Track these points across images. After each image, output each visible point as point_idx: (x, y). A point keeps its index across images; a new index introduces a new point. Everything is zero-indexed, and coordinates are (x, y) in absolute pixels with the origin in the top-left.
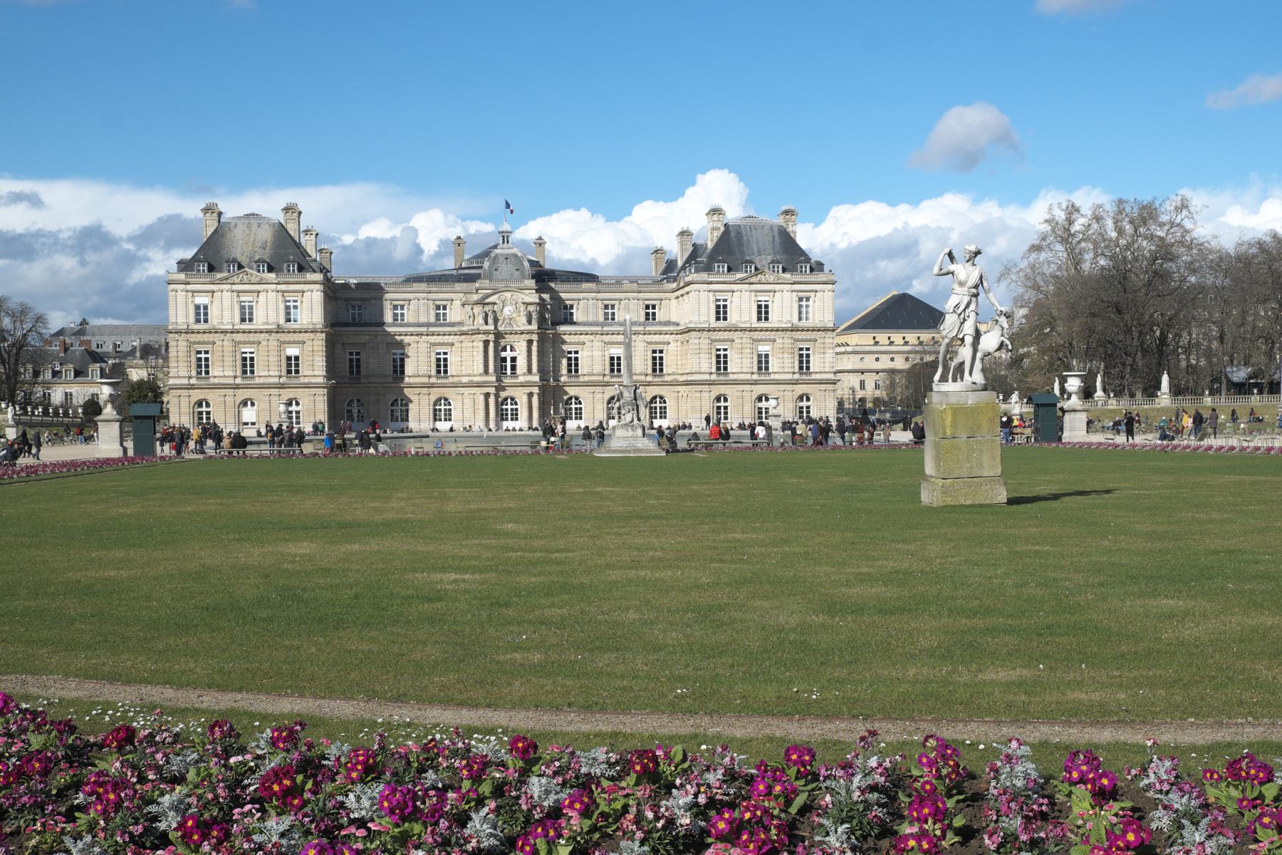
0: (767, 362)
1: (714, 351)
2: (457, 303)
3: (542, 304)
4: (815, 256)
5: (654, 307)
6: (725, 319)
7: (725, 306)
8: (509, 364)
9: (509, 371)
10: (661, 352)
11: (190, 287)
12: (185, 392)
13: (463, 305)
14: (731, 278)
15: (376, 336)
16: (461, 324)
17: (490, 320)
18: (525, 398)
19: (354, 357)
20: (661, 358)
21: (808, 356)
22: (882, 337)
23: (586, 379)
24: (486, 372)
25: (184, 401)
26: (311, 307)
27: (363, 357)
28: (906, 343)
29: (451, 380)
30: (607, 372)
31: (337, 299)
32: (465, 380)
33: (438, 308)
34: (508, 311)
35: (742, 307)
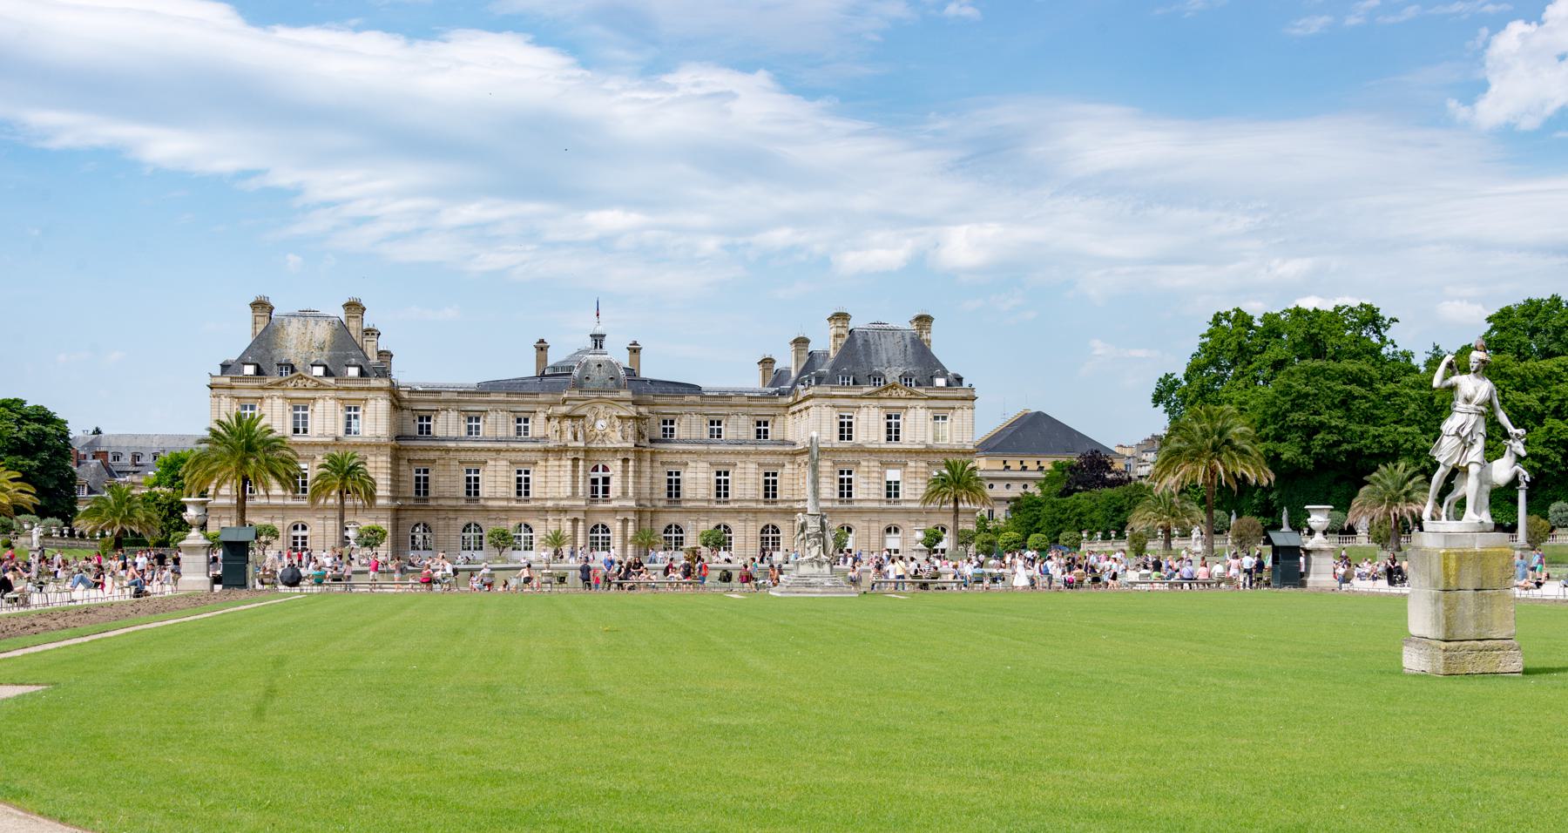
0: (897, 488)
2: (542, 416)
4: (952, 370)
5: (766, 424)
6: (850, 438)
7: (850, 424)
8: (600, 486)
9: (600, 494)
10: (775, 474)
11: (235, 393)
13: (548, 419)
14: (857, 392)
16: (546, 437)
18: (619, 524)
19: (422, 475)
20: (774, 482)
22: (1014, 464)
24: (574, 495)
26: (375, 421)
27: (431, 475)
28: (1041, 468)
29: (532, 504)
30: (713, 497)
32: (549, 504)
33: (519, 421)
34: (601, 424)
35: (869, 426)
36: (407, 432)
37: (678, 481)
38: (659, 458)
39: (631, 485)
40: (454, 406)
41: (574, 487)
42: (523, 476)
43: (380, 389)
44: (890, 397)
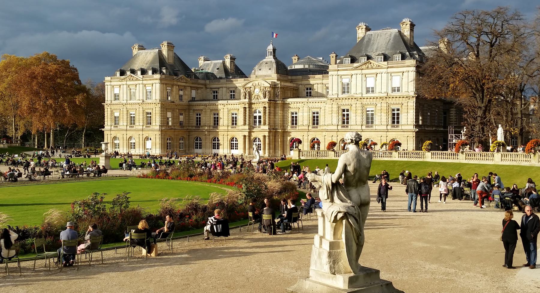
1: (340, 111)
3: (274, 86)
6: (348, 92)
8: (258, 120)
9: (258, 124)
11: (112, 83)
12: (109, 133)
15: (206, 106)
17: (247, 97)
19: (198, 116)
21: (398, 114)
23: (300, 128)
24: (245, 124)
25: (109, 136)
31: (207, 88)
34: (257, 91)
36: (208, 98)
37: (296, 117)
38: (286, 106)
39: (267, 120)
40: (225, 85)
41: (245, 121)
42: (234, 116)
43: (156, 79)
44: (368, 68)
